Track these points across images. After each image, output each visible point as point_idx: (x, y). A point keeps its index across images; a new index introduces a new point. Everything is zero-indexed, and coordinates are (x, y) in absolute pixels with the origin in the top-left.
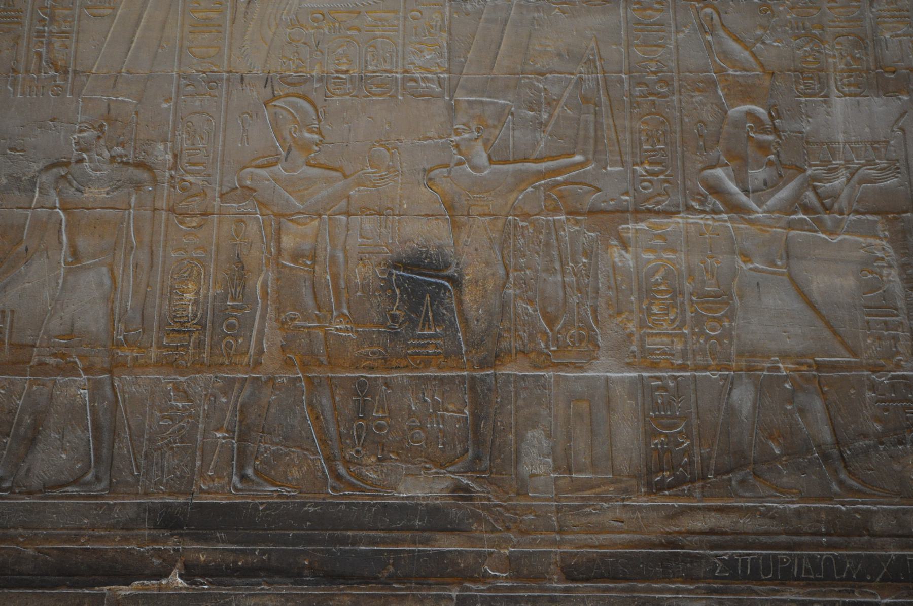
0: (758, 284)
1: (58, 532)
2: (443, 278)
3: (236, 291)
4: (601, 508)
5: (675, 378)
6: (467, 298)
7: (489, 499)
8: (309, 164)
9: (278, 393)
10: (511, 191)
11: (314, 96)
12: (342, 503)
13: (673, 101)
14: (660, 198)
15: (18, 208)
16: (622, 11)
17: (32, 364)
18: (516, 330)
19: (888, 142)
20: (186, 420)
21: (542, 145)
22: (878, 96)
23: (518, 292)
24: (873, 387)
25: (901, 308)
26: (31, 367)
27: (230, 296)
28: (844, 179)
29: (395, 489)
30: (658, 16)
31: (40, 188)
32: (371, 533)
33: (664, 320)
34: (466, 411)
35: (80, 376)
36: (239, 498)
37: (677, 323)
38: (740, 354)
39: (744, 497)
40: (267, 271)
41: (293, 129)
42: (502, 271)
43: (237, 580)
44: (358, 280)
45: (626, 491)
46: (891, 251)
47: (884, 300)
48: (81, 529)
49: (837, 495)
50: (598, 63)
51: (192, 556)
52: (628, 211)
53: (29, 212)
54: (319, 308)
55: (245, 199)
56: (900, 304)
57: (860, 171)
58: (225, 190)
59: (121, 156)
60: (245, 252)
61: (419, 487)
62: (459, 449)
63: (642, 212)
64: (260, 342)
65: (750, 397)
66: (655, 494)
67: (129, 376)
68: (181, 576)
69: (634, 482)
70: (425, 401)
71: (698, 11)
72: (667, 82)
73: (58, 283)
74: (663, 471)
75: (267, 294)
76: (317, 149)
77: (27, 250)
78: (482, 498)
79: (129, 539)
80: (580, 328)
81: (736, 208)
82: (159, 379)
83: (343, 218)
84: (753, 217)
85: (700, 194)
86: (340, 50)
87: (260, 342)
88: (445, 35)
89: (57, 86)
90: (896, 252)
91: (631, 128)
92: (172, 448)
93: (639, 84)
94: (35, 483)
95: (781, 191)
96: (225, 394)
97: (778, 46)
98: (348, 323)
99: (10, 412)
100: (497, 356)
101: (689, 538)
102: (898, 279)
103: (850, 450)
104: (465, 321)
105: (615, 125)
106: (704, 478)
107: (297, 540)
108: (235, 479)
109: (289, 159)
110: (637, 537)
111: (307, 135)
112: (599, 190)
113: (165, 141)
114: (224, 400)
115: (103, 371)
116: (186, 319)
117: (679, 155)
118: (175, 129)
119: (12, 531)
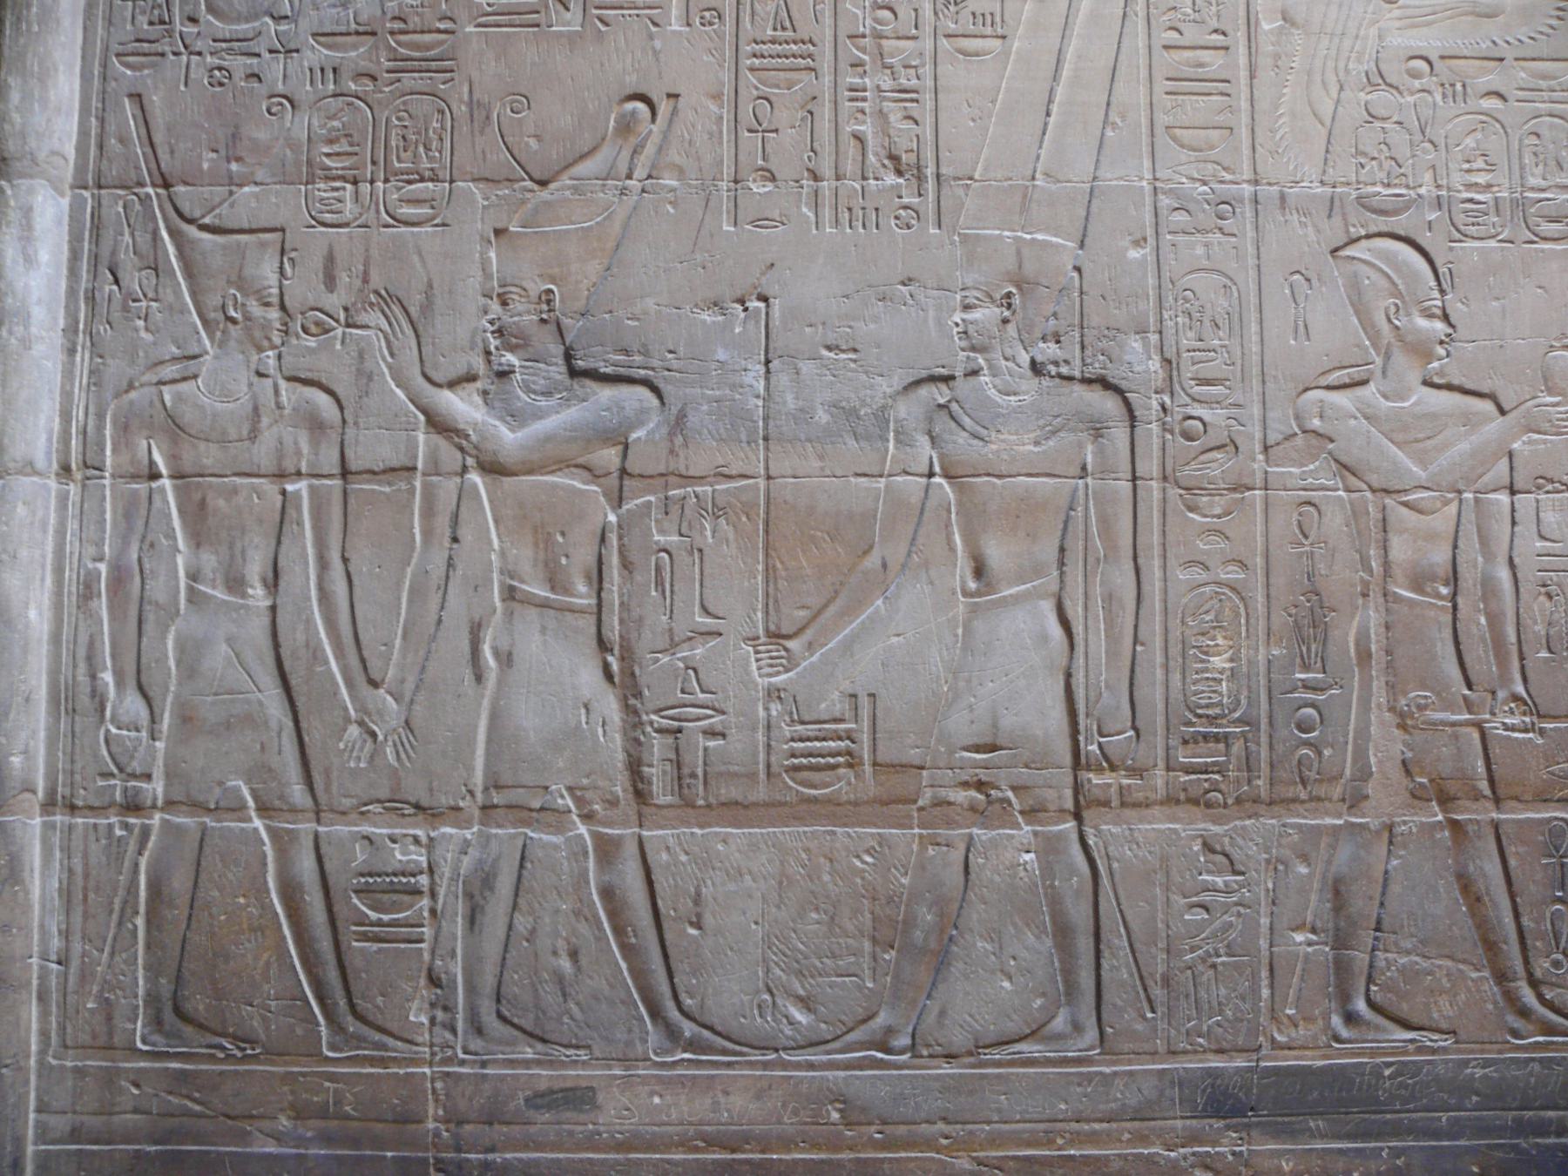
1: (1014, 1126)
3: (1309, 650)
8: (1427, 383)
9: (1402, 853)
11: (1425, 239)
12: (1533, 1059)
15: (857, 475)
17: (920, 803)
20: (1235, 909)
26: (921, 809)
27: (1298, 660)
31: (897, 433)
35: (1017, 826)
36: (1346, 1056)
40: (1365, 607)
41: (1393, 309)
54: (1470, 687)
55: (1315, 458)
60: (1322, 567)
67: (1115, 824)
73: (956, 635)
75: (1370, 655)
76: (1441, 351)
77: (884, 566)
79: (1147, 1137)
82: (1175, 831)
83: (1504, 497)
86: (1470, 142)
87: (1361, 755)
89: (906, 207)
92: (1214, 966)
94: (959, 1039)
96: (1305, 858)
98: (1524, 714)
99: (890, 900)
107: (1455, 1130)
108: (1336, 1021)
109: (1389, 373)
111: (1422, 323)
113: (1142, 331)
114: (1303, 870)
116: (1217, 711)
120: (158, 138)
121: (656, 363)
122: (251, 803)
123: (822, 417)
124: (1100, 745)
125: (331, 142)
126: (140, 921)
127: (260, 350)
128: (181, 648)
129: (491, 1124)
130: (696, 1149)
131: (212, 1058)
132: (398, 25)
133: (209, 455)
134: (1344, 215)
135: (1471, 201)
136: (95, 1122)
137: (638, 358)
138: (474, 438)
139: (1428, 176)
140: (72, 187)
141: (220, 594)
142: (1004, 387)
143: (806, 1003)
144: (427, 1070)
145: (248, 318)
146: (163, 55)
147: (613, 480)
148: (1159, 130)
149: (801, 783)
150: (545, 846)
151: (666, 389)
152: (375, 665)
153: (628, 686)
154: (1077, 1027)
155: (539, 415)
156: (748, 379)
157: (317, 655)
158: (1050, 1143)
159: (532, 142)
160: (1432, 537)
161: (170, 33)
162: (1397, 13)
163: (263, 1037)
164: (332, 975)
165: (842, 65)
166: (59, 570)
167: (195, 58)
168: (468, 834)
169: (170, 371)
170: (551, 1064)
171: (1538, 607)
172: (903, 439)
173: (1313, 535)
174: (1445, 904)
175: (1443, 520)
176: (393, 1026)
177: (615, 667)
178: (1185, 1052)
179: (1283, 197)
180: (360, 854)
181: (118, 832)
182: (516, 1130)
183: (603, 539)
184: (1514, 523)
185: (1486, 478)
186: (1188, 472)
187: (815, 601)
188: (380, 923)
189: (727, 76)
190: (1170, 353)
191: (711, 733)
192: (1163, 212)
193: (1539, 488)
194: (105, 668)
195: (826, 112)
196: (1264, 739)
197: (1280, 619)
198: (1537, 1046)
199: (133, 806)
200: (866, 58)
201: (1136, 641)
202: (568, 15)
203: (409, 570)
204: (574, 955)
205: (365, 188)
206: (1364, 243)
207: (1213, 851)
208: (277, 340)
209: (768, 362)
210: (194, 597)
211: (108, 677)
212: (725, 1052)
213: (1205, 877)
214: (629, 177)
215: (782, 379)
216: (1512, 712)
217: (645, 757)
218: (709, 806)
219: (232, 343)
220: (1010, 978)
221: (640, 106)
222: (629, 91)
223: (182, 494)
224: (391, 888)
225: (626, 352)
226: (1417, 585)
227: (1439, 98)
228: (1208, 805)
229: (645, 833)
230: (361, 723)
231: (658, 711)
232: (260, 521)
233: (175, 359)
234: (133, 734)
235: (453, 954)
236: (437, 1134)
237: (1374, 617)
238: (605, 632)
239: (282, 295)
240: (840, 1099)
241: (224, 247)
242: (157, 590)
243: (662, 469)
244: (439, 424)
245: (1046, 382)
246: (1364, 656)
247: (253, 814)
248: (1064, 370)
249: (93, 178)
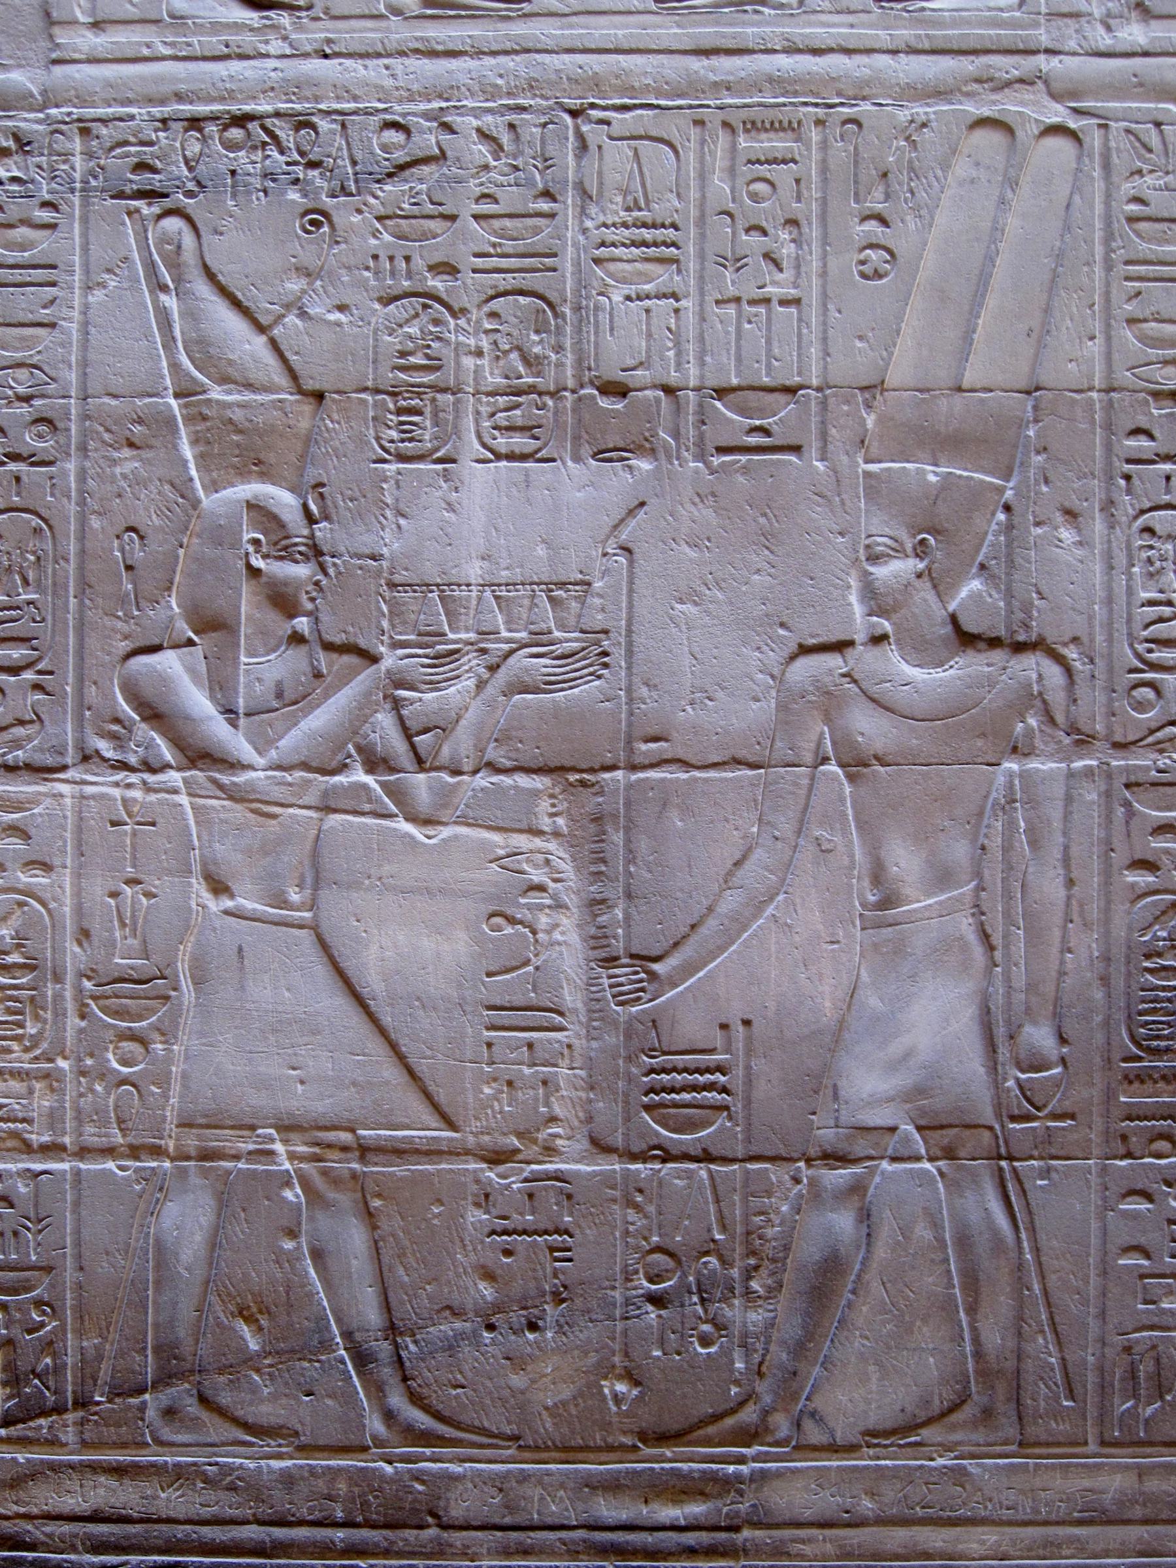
0: (240, 949)
13: (64, 474)
14: (19, 731)
19: (589, 584)
22: (577, 459)
24: (485, 1199)
25: (575, 1011)
28: (471, 683)
38: (186, 1124)
39: (172, 1444)
46: (567, 868)
47: (534, 990)
49: (379, 1443)
56: (571, 998)
57: (511, 661)
65: (203, 1220)
81: (200, 756)
84: (241, 778)
85: (117, 720)
90: (578, 869)
95: (317, 712)
97: (338, 324)
101: (48, 1529)
102: (574, 938)
103: (416, 1342)
106: (82, 1403)
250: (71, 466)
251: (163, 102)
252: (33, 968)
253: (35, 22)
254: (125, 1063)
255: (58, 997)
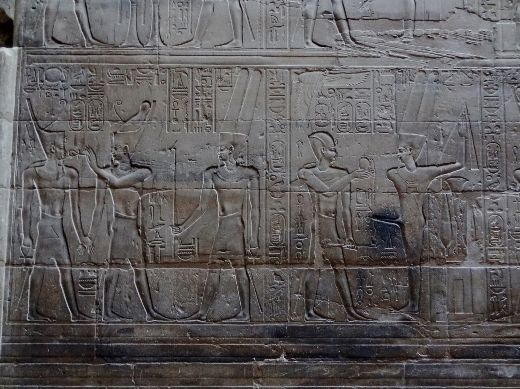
2: (396, 222)
4: (468, 328)
5: (501, 269)
6: (407, 233)
7: (419, 324)
8: (331, 167)
10: (426, 181)
11: (331, 132)
13: (502, 136)
14: (495, 184)
16: (478, 89)
18: (430, 247)
21: (441, 158)
23: (430, 229)
26: (209, 264)
29: (377, 319)
30: (496, 93)
32: (367, 339)
33: (497, 243)
34: (408, 284)
35: (231, 268)
37: (502, 244)
42: (423, 219)
43: (310, 359)
44: (357, 224)
45: (479, 319)
48: (239, 337)
50: (467, 116)
51: (289, 349)
52: (480, 190)
53: (201, 190)
54: (339, 237)
55: (302, 184)
58: (292, 179)
59: (242, 163)
60: (303, 210)
61: (388, 320)
62: (405, 302)
63: (487, 191)
64: (312, 253)
66: (491, 321)
68: (285, 357)
69: (482, 316)
70: (389, 280)
71: (515, 90)
72: (499, 126)
74: (495, 311)
76: (334, 159)
78: (414, 323)
80: (459, 246)
82: (268, 270)
83: (348, 193)
85: (514, 182)
86: (343, 109)
87: (312, 253)
88: (394, 101)
89: (208, 127)
91: (483, 149)
92: (277, 302)
93: (487, 127)
94: (217, 317)
96: (299, 277)
99: (202, 285)
100: (421, 260)
104: (406, 243)
105: (475, 148)
106: (512, 314)
108: (306, 315)
110: (483, 339)
111: (329, 152)
112: (467, 180)
113: (262, 155)
114: (298, 280)
115: (242, 266)
117: (505, 163)
118: (266, 149)
119: (209, 338)
120: (34, 109)
121: (150, 163)
122: (56, 263)
123: (188, 175)
124: (251, 250)
125: (75, 111)
126: (29, 291)
127: (59, 159)
128: (40, 228)
129: (109, 337)
130: (156, 343)
131: (45, 322)
132: (90, 84)
133: (47, 184)
134: (312, 127)
135: (343, 123)
136: (16, 338)
137: (146, 162)
138: (109, 180)
139: (332, 118)
140: (14, 120)
141: (50, 215)
142: (230, 169)
143: (182, 308)
144: (95, 324)
145: (56, 152)
146: (35, 89)
147: (141, 190)
148: (268, 108)
149: (182, 258)
150: (124, 272)
151: (153, 169)
152: (85, 231)
153: (143, 236)
154: (245, 315)
155: (124, 175)
156: (171, 167)
157: (72, 229)
158: (238, 342)
159: (123, 112)
160: (330, 202)
161: (37, 84)
162: (327, 78)
163: (57, 317)
164: (73, 302)
165: (194, 94)
166: (10, 210)
167: (43, 90)
168: (106, 270)
169: (37, 164)
170: (124, 322)
171: (356, 219)
172: (206, 180)
173: (301, 202)
174: (332, 289)
175: (332, 199)
176: (88, 314)
177: (140, 232)
178: (270, 322)
179: (297, 123)
180: (81, 275)
181: (24, 270)
182: (115, 338)
183: (138, 203)
184: (351, 199)
185: (345, 189)
186: (272, 188)
187: (186, 217)
188: (85, 290)
189: (167, 96)
190: (268, 160)
191: (162, 247)
192: (268, 128)
193: (357, 191)
194: (22, 232)
195: (190, 105)
196: (289, 249)
197: (294, 221)
198: (355, 323)
199: (28, 264)
200: (199, 92)
201: (259, 226)
202: (130, 82)
203: (94, 210)
204: (130, 297)
205: (84, 122)
206: (316, 134)
207: (277, 275)
208: (63, 157)
209: (175, 163)
210: (43, 216)
211: (22, 234)
212: (163, 320)
213: (276, 281)
214: (145, 120)
215: (179, 167)
216: (349, 244)
217: (147, 252)
218: (161, 263)
219: (52, 158)
220: (229, 303)
221: (147, 104)
222: (145, 100)
223: (41, 193)
224: (88, 282)
225: (143, 161)
226: (327, 213)
227: (336, 98)
228: (276, 264)
229: (147, 269)
230: (82, 245)
231: (150, 242)
232: (59, 199)
233: (39, 161)
234: (28, 247)
235: (102, 297)
236: (97, 339)
237: (316, 221)
238: (139, 224)
239: (64, 147)
240: (189, 331)
241: (51, 135)
242: (34, 214)
243: (151, 187)
244: (101, 177)
245: (239, 167)
246: (313, 230)
247: (57, 265)
248: (243, 165)
249: (19, 118)
250: (503, 134)
251: (516, 66)
252: (499, 229)
253: (492, 50)
254: (518, 247)
255: (505, 235)
